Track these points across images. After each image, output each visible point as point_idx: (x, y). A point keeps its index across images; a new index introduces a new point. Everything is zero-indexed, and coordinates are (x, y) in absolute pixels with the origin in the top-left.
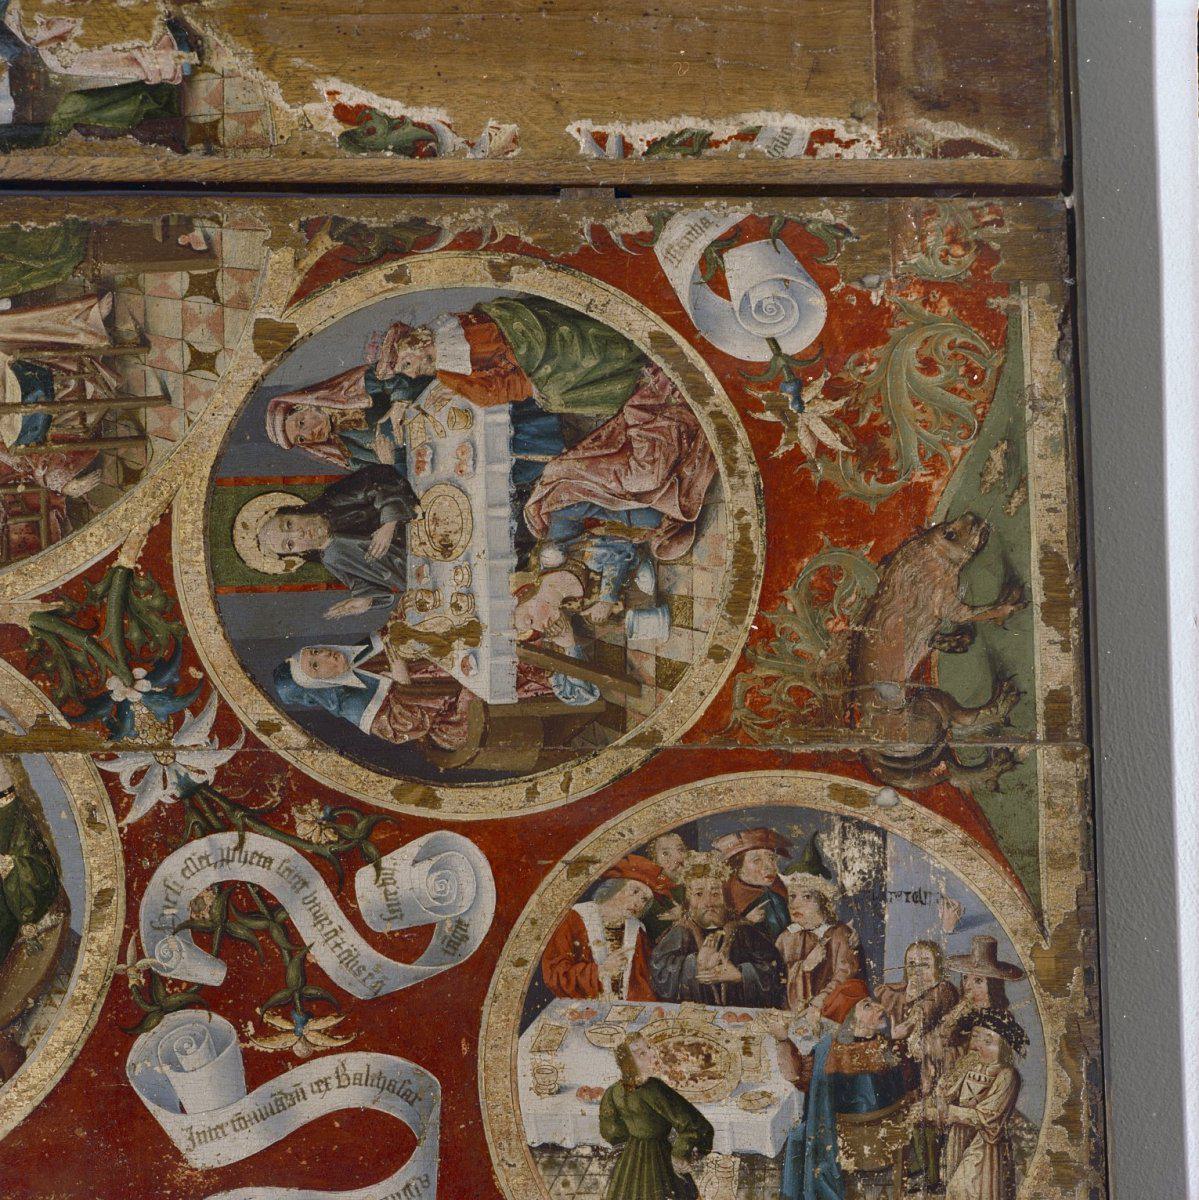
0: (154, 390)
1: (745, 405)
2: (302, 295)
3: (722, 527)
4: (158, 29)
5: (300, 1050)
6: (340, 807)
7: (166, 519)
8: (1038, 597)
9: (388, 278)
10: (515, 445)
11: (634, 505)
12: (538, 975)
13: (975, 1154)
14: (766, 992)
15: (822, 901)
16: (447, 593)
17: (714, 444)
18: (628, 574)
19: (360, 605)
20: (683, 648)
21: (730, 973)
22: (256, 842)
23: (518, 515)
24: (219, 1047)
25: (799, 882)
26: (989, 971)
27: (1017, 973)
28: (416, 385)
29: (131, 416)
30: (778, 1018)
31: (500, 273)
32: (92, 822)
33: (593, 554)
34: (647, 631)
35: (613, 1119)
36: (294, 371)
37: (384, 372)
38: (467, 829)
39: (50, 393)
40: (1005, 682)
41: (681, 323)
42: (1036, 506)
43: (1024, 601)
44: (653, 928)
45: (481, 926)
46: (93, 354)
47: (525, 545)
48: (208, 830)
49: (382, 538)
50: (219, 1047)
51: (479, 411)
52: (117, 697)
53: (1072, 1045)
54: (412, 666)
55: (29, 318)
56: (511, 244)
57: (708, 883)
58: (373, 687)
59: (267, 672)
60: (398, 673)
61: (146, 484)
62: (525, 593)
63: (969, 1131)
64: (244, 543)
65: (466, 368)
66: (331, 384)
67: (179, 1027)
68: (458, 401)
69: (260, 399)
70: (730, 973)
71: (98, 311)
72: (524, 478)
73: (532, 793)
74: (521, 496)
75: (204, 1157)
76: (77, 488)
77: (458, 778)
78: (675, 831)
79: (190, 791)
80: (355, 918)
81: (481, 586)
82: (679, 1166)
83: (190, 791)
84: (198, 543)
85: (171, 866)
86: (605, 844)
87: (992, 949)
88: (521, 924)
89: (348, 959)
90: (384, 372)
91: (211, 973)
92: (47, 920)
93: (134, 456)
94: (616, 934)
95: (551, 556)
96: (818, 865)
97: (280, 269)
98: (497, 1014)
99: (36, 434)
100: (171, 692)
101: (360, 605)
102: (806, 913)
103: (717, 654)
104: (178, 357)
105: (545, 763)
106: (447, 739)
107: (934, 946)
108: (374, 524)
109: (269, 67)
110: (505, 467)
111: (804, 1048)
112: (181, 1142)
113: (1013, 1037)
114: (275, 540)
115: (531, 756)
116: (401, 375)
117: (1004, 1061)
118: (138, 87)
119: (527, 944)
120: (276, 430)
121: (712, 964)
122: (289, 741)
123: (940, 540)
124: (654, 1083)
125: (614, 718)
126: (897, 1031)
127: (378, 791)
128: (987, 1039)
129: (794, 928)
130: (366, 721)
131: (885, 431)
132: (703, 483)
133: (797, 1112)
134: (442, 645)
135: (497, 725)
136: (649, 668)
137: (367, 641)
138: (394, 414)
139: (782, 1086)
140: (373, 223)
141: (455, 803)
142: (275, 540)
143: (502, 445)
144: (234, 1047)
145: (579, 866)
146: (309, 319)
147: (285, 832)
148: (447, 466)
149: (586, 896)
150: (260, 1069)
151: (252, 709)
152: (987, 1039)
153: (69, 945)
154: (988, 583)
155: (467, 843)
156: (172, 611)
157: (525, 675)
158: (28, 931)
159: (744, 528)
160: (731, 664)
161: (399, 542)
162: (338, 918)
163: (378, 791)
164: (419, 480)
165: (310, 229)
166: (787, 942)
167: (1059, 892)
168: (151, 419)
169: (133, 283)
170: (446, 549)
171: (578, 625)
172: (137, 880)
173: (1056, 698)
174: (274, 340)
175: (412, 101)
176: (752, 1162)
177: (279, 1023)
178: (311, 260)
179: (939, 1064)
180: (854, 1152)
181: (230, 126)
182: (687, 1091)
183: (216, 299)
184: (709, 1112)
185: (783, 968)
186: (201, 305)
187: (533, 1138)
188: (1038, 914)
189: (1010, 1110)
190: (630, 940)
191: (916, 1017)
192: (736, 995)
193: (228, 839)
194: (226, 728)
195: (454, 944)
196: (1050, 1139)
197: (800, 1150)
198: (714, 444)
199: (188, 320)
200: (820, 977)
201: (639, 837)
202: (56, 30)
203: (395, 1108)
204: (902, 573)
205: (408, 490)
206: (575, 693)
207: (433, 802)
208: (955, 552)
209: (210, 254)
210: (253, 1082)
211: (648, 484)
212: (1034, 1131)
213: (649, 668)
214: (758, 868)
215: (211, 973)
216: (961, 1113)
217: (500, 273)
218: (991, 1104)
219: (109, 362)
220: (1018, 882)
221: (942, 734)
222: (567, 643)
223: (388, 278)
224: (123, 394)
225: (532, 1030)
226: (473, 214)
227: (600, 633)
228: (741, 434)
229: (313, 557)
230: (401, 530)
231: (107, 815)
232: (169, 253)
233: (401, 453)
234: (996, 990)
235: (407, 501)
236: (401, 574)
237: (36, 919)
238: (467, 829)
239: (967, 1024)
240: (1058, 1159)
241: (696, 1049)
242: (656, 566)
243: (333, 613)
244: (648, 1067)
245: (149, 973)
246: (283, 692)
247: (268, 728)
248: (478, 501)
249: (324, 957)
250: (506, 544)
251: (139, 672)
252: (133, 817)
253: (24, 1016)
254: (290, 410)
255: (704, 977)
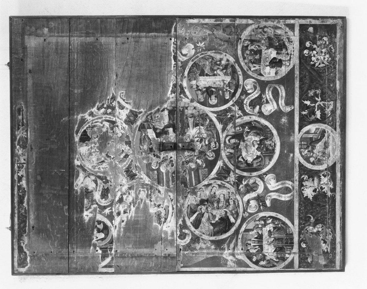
0: (198, 113)
1: (199, 52)
2: (188, 98)
3: (212, 55)
4: (162, 113)
5: (266, 98)
6: (241, 94)
7: (211, 112)
8: (220, 22)
9: (186, 89)
10: (204, 76)
11: (210, 64)
12: (258, 75)
13: (277, 31)
14: (260, 52)
15: (251, 46)
16: (219, 83)
17: (204, 55)
18: (217, 64)
19: (221, 92)
20: (225, 59)
21: (258, 55)
22: (245, 102)
23: (211, 76)
24: (265, 106)
25: (249, 48)
26: (258, 29)
27: (259, 26)
28: (197, 86)
29: (201, 115)
30: (263, 50)
31: (185, 77)
32: (243, 119)
33: (215, 68)
34: (223, 62)
35: (272, 67)
36: (196, 98)
37: (196, 89)
38: (244, 82)
39: (198, 123)
40: (228, 26)
41: (190, 59)
42: (210, 22)
43: (220, 24)
44: (253, 63)
45: (253, 80)
46: (194, 119)
47: (214, 75)
48: (243, 107)
49: (213, 90)
50: (265, 106)
51: (200, 80)
52: (230, 116)
53: (266, 21)
54: (227, 87)
55: (190, 126)
56: (182, 76)
57: (249, 57)
58: (229, 91)
59: (227, 101)
60: (228, 88)
61: (208, 113)
62: (219, 75)
63: (274, 32)
64: (214, 104)
65: (195, 81)
66: (197, 95)
67: (263, 110)
68: (199, 82)
69: (199, 102)
70: (258, 55)
71: (190, 119)
72: (207, 75)
73: (240, 75)
74: (209, 76)
75: (276, 107)
76: (208, 121)
77: (238, 82)
78: (244, 60)
79: (239, 109)
80: (253, 93)
81: (218, 80)
82: (278, 61)
83: (239, 109)
84: (214, 108)
85: (247, 111)
86: (245, 68)
87: (256, 29)
88: (253, 76)
89: (257, 93)
90: (196, 89)
91: (258, 107)
92: (252, 123)
93: (205, 115)
94: (254, 67)
95: (215, 72)
96: (247, 46)
97: (185, 100)
98: (262, 79)
99: (202, 125)
100: (230, 111)
101: (221, 92)
102: (253, 47)
103: (226, 55)
104: (194, 111)
105: (237, 74)
106: (234, 83)
107: (256, 35)
108: (212, 90)
109: (167, 101)
110: (206, 77)
111: (266, 48)
112: (275, 110)
113: (265, 27)
114: (214, 101)
115: (236, 75)
116: (196, 88)
117: (267, 28)
118: (168, 115)
119: (255, 76)
120: (202, 100)
121: (257, 57)
122: (235, 99)
123: (214, 32)
124: (269, 63)
125: (233, 66)
126: (264, 39)
127: (240, 91)
128: (266, 29)
129: (254, 49)
130: (233, 91)
131: (202, 37)
132: (207, 56)
133: (273, 49)
134: (224, 84)
135: (233, 78)
136: (227, 62)
137: (224, 91)
138: (200, 88)
139: (270, 50)
140: (180, 91)
141: (241, 82)
142: (214, 101)
143: (204, 77)
144: (265, 105)
145: (247, 70)
146: (190, 97)
147: (244, 99)
148: (206, 83)
149: (250, 69)
150: (267, 102)
151: (231, 103)
152: (266, 29)
153: (255, 121)
154: (218, 27)
155: (245, 81)
156: (221, 111)
157: (228, 75)
158: (253, 125)
159: (212, 53)
160: (227, 54)
161: (214, 88)
162: (252, 94)
163: (240, 91)
164: (207, 86)
165: (180, 97)
166: (255, 49)
167: (250, 21)
168: (201, 113)
169: (186, 115)
170: (215, 83)
171: (222, 70)
172: (249, 114)
173: (231, 21)
174: (192, 101)
175: (170, 86)
176: (277, 53)
177: (263, 100)
178: (184, 97)
179: (268, 34)
180: (276, 43)
181: (173, 105)
182: (270, 60)
183: (188, 107)
184: (272, 58)
185: (258, 50)
186: (189, 108)
187: (275, 75)
188: (253, 24)
189: (272, 27)
190: (255, 65)
191: (263, 37)
192: (261, 54)
193: (245, 105)
194: (233, 105)
195: (255, 83)
196: (275, 23)
197: (276, 48)
198: (204, 55)
199: (190, 110)
200: (259, 46)
201: (245, 64)
202: (163, 123)
203: (271, 89)
204: (218, 37)
205: (208, 87)
206: (229, 70)
207: (241, 85)
208: (215, 31)
209: (183, 107)
210: (269, 103)
211: (208, 62)
212: (274, 25)
213: (227, 62)
214: (248, 52)
215: (258, 107)
216: (273, 32)
217: (185, 77)
218: (272, 29)
219: (195, 117)
220: (249, 26)
221: (234, 33)
222: (224, 71)
223: (186, 89)
224: (198, 116)
225: (264, 75)
226: (179, 80)
227: (223, 67)
228: (203, 52)
229: (215, 97)
230: (213, 88)
231: (242, 118)
232: (183, 112)
233: (205, 88)
234: (260, 28)
235: (210, 87)
236: (217, 88)
237: (252, 124)
238: (244, 82)
239: (264, 32)
240: (277, 23)
241: (266, 59)
242: (217, 62)
243: (221, 95)
244: (268, 64)
245: (258, 113)
246: (230, 100)
247: (233, 101)
248: (210, 80)
249: (257, 96)
250: (214, 77)
251: (227, 114)
252: (242, 115)
253: (262, 125)
254: (200, 99)
255: (259, 58)
